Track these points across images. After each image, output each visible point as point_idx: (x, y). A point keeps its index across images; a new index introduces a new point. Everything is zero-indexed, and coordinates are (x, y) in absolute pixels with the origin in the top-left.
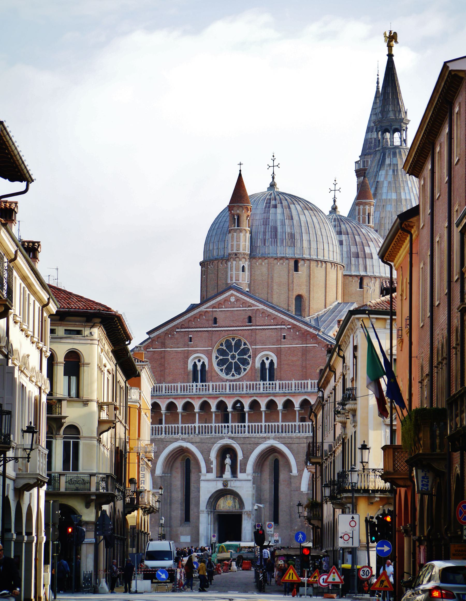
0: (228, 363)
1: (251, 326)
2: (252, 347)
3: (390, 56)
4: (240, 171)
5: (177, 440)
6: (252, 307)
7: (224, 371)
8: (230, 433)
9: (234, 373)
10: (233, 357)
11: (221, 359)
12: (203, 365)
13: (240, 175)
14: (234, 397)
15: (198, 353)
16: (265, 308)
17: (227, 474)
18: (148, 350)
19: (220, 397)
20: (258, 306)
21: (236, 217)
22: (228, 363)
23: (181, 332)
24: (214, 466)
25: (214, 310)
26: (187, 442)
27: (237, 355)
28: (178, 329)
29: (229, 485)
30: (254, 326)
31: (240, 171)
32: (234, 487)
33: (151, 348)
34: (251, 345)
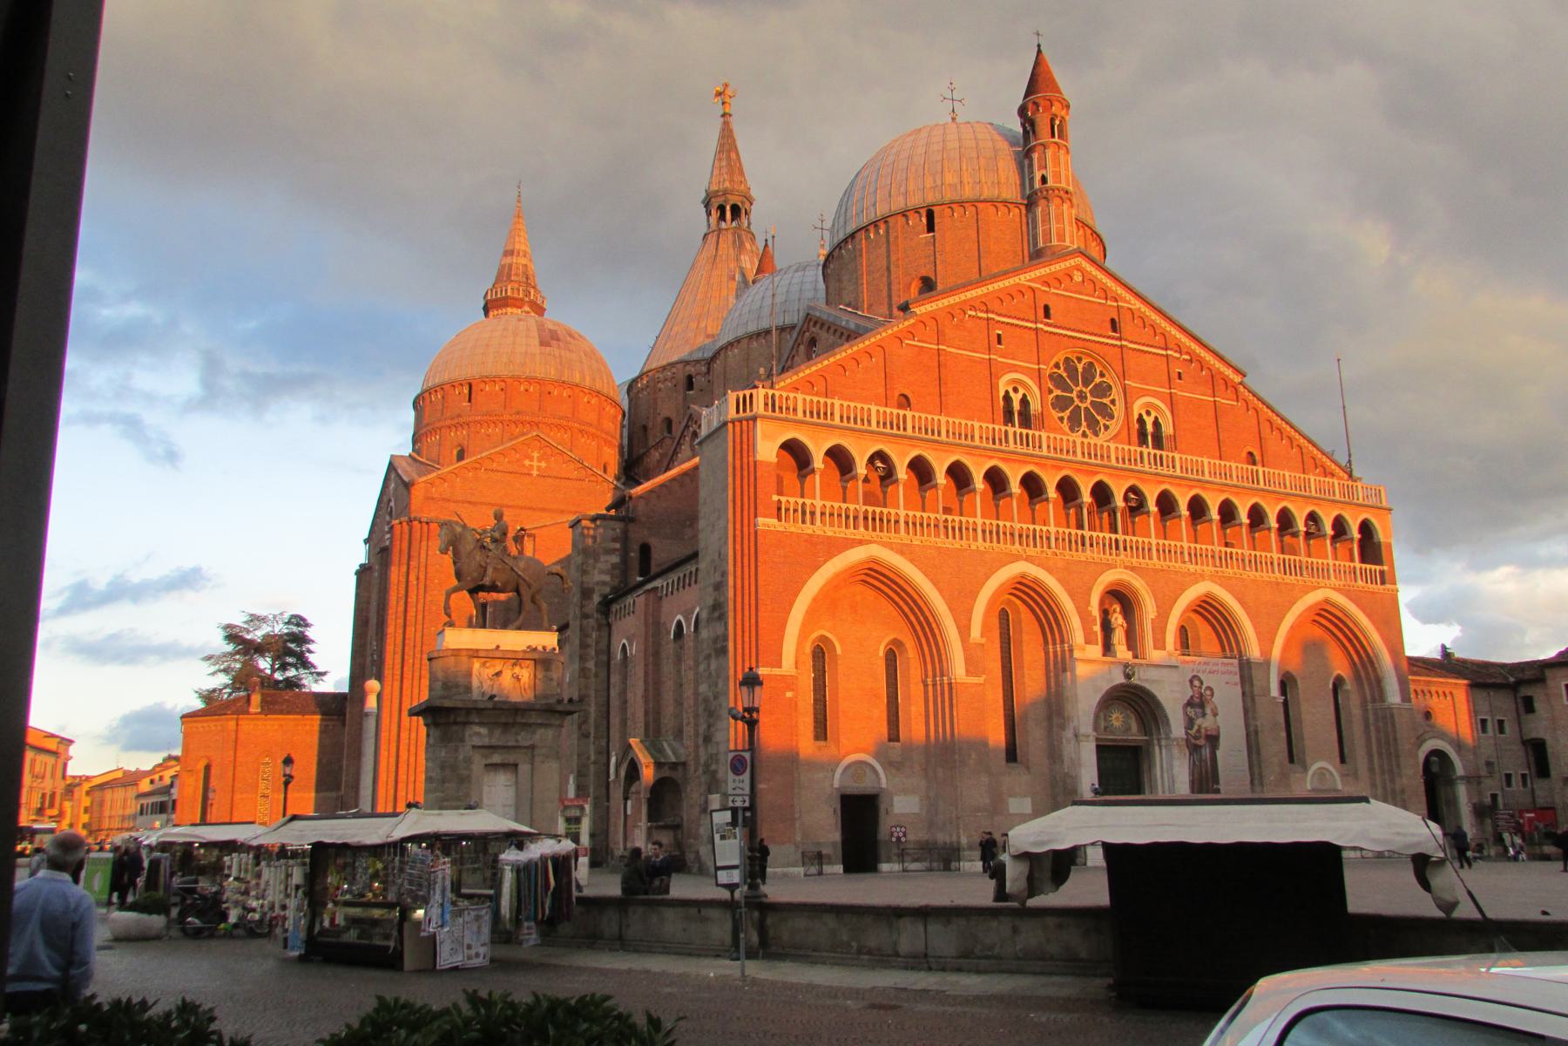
1: (1120, 339)
2: (1127, 382)
4: (1039, 46)
5: (1015, 558)
6: (1116, 301)
7: (1065, 421)
8: (1122, 556)
10: (1082, 397)
11: (1057, 396)
12: (1024, 402)
13: (1039, 52)
14: (1128, 478)
15: (1016, 371)
16: (1144, 309)
17: (1122, 652)
18: (907, 342)
20: (1128, 302)
23: (980, 318)
24: (1097, 628)
25: (1044, 288)
26: (1038, 566)
27: (1088, 395)
29: (1136, 676)
30: (1125, 340)
31: (1039, 46)
32: (1147, 680)
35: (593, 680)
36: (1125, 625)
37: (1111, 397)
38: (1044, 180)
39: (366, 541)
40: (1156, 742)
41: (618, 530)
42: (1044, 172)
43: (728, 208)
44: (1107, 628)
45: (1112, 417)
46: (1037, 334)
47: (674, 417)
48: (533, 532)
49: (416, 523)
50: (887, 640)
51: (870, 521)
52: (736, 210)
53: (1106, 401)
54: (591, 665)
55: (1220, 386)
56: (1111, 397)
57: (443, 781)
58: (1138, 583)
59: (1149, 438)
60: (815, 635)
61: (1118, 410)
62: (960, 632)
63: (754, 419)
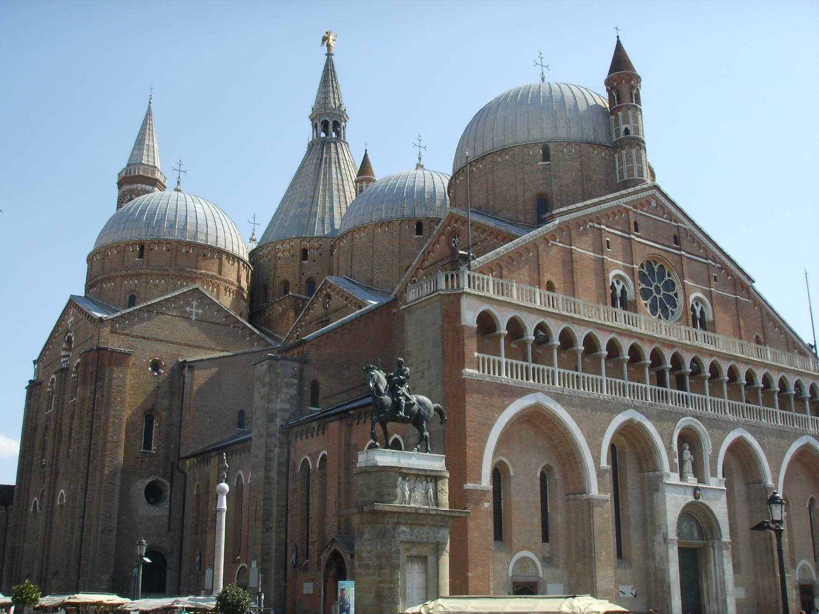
0: (652, 297)
1: (680, 250)
2: (685, 281)
3: (329, 55)
4: (618, 37)
6: (677, 223)
9: (661, 315)
10: (658, 291)
11: (642, 288)
12: (623, 291)
16: (694, 229)
19: (675, 346)
21: (635, 92)
22: (652, 297)
23: (595, 227)
24: (677, 460)
26: (641, 413)
28: (590, 221)
30: (684, 251)
31: (618, 37)
33: (558, 240)
34: (682, 277)
35: (276, 486)
36: (692, 459)
37: (675, 292)
38: (627, 131)
39: (35, 362)
40: (710, 544)
41: (296, 369)
42: (627, 126)
43: (331, 123)
44: (682, 462)
45: (675, 306)
46: (631, 243)
47: (290, 279)
48: (192, 364)
49: (102, 352)
50: (542, 466)
51: (536, 374)
52: (336, 125)
53: (672, 294)
54: (273, 474)
55: (739, 288)
56: (675, 292)
57: (380, 567)
58: (701, 428)
59: (698, 322)
60: (496, 460)
61: (680, 301)
62: (595, 462)
63: (460, 295)
